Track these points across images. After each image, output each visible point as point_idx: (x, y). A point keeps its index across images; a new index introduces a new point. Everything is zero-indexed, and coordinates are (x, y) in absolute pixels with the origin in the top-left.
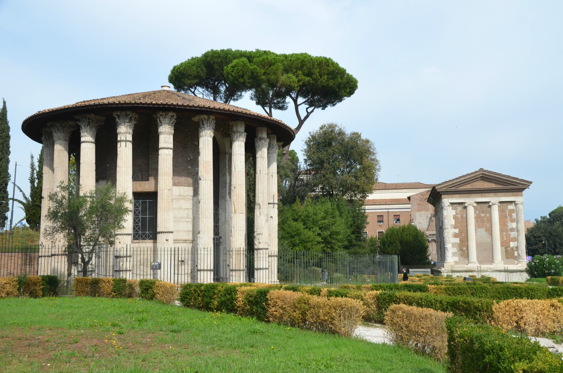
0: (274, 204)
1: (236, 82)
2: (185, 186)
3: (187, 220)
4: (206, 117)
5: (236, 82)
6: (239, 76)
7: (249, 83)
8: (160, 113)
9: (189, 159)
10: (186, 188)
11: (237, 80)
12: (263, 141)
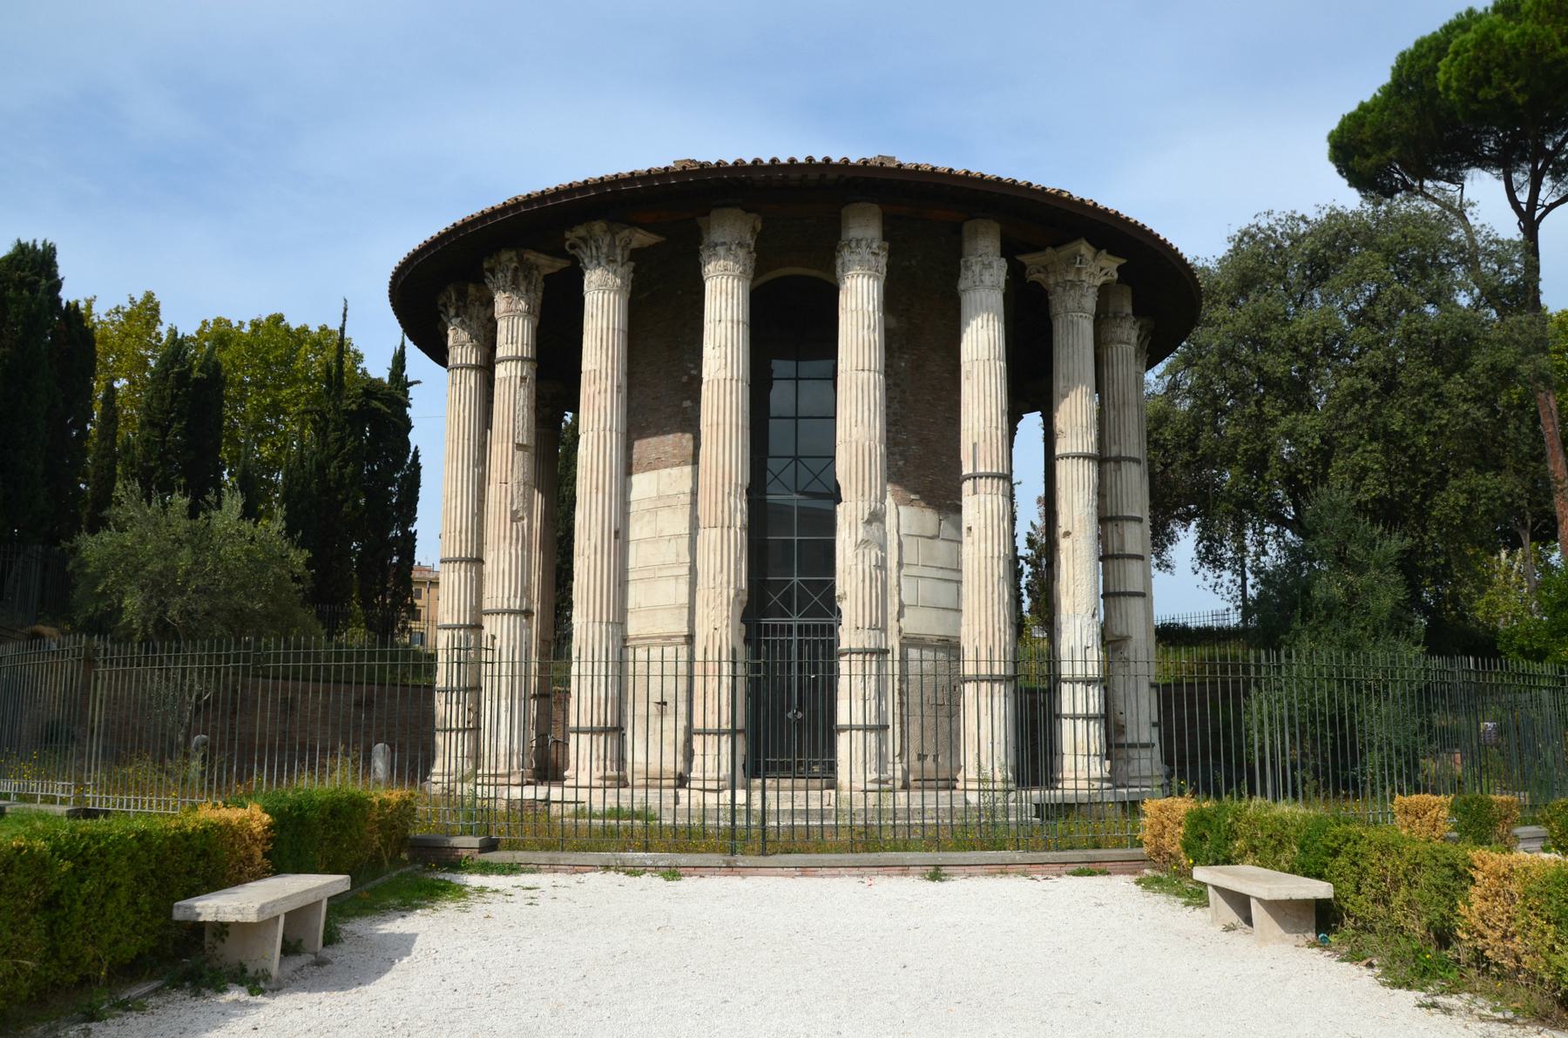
0: (974, 477)
1: (1474, 107)
2: (673, 465)
3: (676, 572)
4: (581, 231)
5: (1474, 107)
6: (1478, 83)
7: (1517, 90)
8: (486, 265)
9: (685, 379)
10: (675, 471)
11: (1474, 98)
12: (846, 252)
